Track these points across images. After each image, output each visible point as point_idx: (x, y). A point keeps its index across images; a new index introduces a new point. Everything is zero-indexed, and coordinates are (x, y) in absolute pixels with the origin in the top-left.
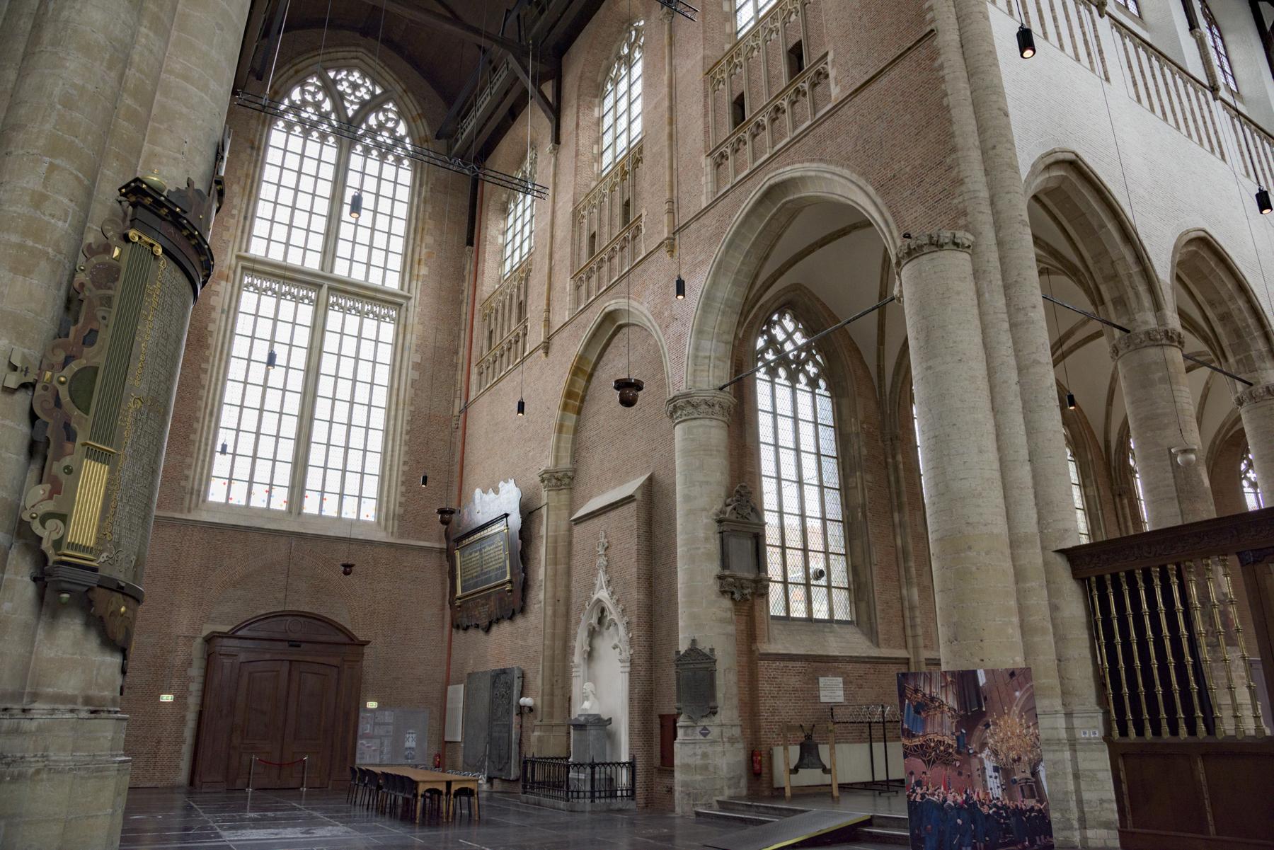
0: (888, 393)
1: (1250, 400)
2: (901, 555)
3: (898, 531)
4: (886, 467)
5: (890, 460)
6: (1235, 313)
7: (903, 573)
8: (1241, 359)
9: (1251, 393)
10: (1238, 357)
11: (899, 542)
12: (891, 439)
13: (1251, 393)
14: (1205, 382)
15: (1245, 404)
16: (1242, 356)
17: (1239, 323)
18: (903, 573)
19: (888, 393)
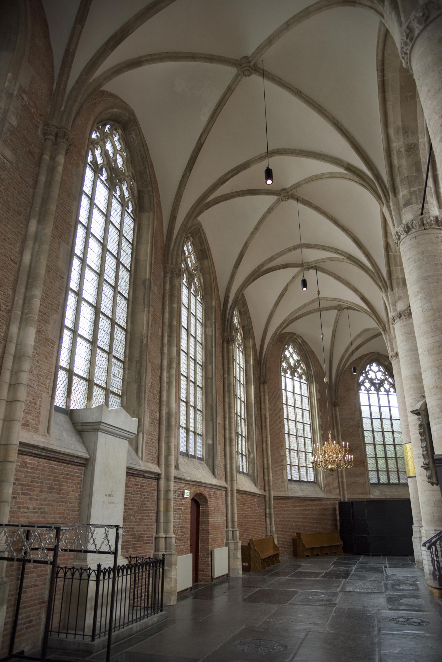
0: (69, 88)
1: (419, 227)
2: (23, 277)
3: (30, 243)
4: (39, 164)
5: (46, 157)
6: (421, 146)
7: (19, 300)
8: (415, 191)
9: (422, 220)
10: (412, 189)
11: (27, 258)
12: (57, 134)
13: (422, 220)
14: (286, 284)
15: (413, 230)
16: (416, 189)
17: (421, 157)
18: (19, 300)
19: (69, 88)
